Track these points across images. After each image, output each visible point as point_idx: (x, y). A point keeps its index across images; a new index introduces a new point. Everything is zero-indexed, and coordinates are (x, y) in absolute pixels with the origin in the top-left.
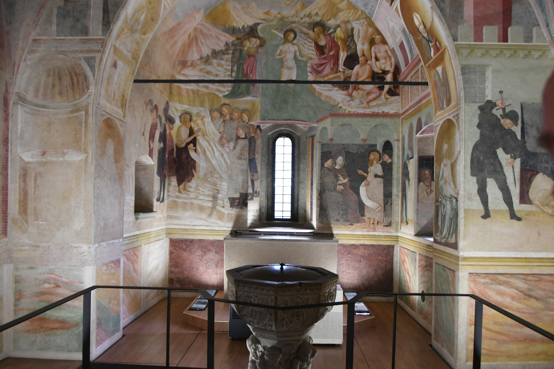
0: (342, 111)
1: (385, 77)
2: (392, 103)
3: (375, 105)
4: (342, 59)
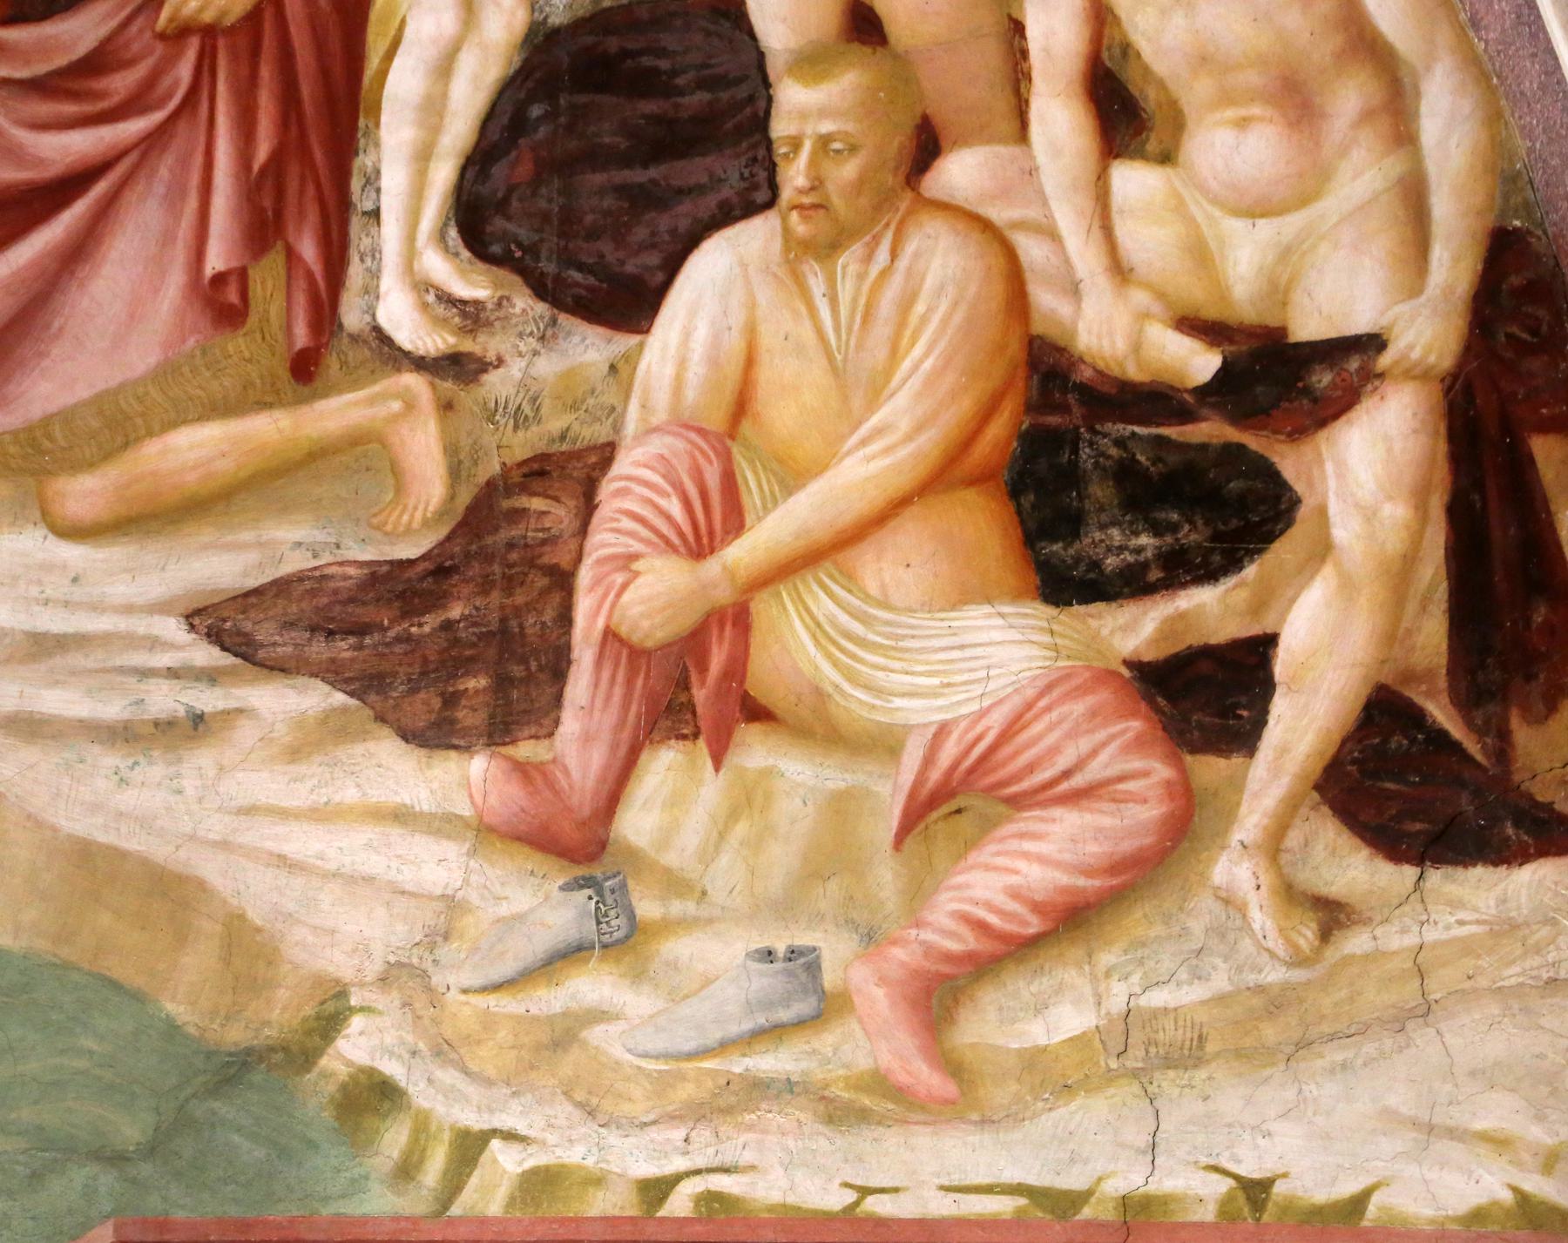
0: (406, 1171)
1: (1289, 462)
2: (1426, 1011)
3: (1078, 1042)
4: (433, 109)
